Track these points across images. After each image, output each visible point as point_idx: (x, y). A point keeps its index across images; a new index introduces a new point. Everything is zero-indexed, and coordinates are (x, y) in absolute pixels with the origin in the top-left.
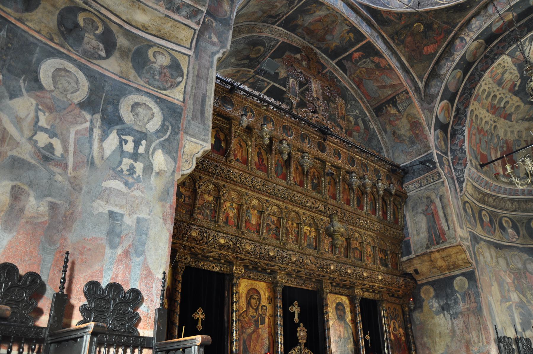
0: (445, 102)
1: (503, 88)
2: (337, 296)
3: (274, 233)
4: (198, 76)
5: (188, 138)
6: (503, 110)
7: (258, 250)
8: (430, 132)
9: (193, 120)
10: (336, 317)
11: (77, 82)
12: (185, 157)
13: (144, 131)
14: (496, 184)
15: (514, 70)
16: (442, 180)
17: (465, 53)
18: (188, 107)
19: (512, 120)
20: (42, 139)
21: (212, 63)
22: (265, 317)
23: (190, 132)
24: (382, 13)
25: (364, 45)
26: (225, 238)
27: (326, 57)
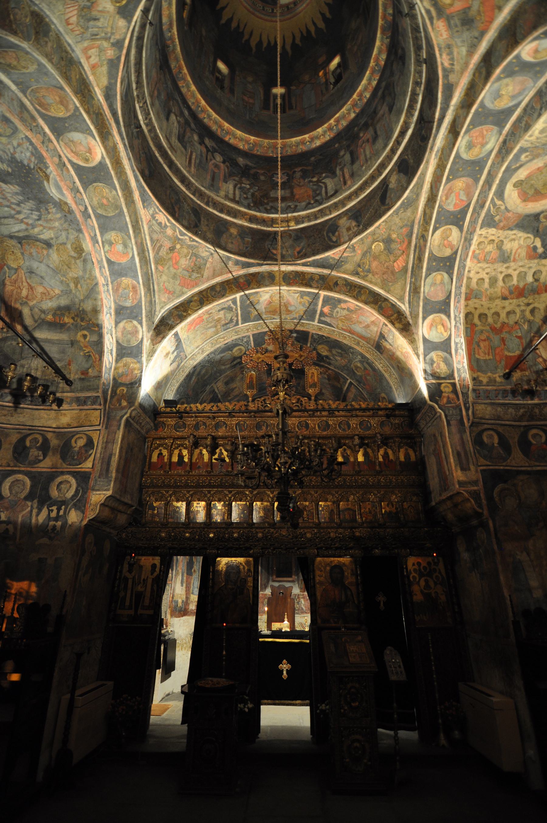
0: (431, 317)
1: (514, 260)
2: (332, 559)
5: (94, 493)
6: (536, 284)
7: (221, 535)
8: (419, 359)
9: (99, 477)
11: (24, 484)
12: (92, 507)
13: (64, 499)
15: (515, 234)
16: (438, 414)
18: (96, 469)
21: (120, 425)
23: (96, 488)
24: (332, 256)
26: (190, 533)
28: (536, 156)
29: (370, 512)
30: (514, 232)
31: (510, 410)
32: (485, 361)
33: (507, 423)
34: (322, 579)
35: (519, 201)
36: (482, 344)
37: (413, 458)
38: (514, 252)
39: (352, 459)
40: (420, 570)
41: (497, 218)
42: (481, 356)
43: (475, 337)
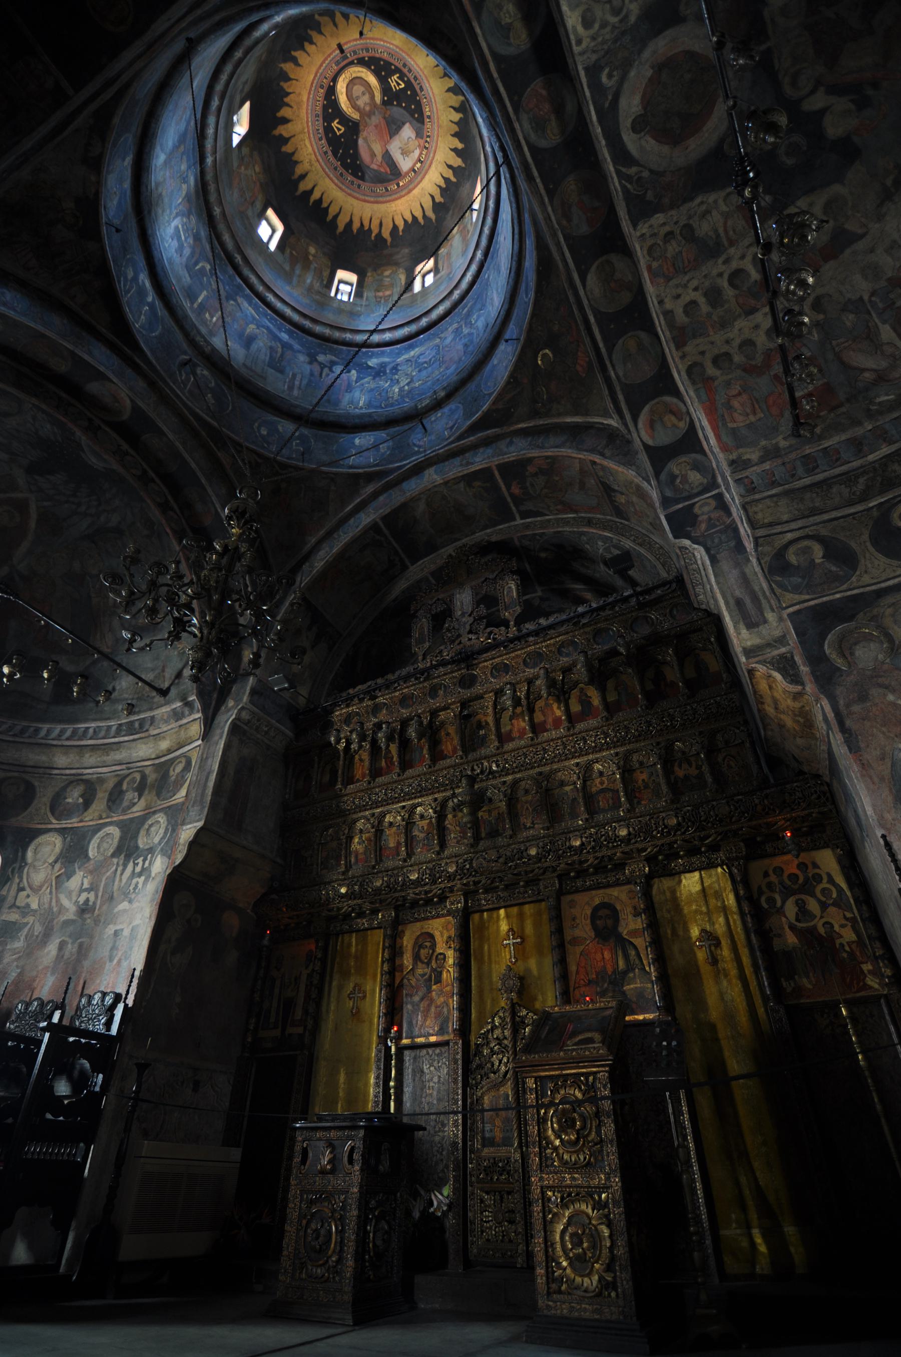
0: (647, 408)
1: (732, 243)
2: (594, 892)
3: (424, 845)
4: (207, 758)
5: (184, 828)
7: (392, 880)
9: (193, 806)
10: (593, 934)
12: (180, 849)
14: (895, 415)
15: (702, 203)
17: (596, 312)
19: (860, 231)
20: (84, 896)
21: (223, 732)
22: (441, 973)
25: (500, 474)
27: (506, 525)
28: (626, 66)
29: (646, 786)
30: (698, 200)
31: (834, 490)
32: (750, 426)
33: (834, 514)
34: (577, 932)
35: (666, 149)
36: (735, 403)
37: (714, 664)
38: (721, 231)
39: (596, 701)
40: (781, 883)
41: (650, 195)
42: (740, 421)
43: (717, 398)
